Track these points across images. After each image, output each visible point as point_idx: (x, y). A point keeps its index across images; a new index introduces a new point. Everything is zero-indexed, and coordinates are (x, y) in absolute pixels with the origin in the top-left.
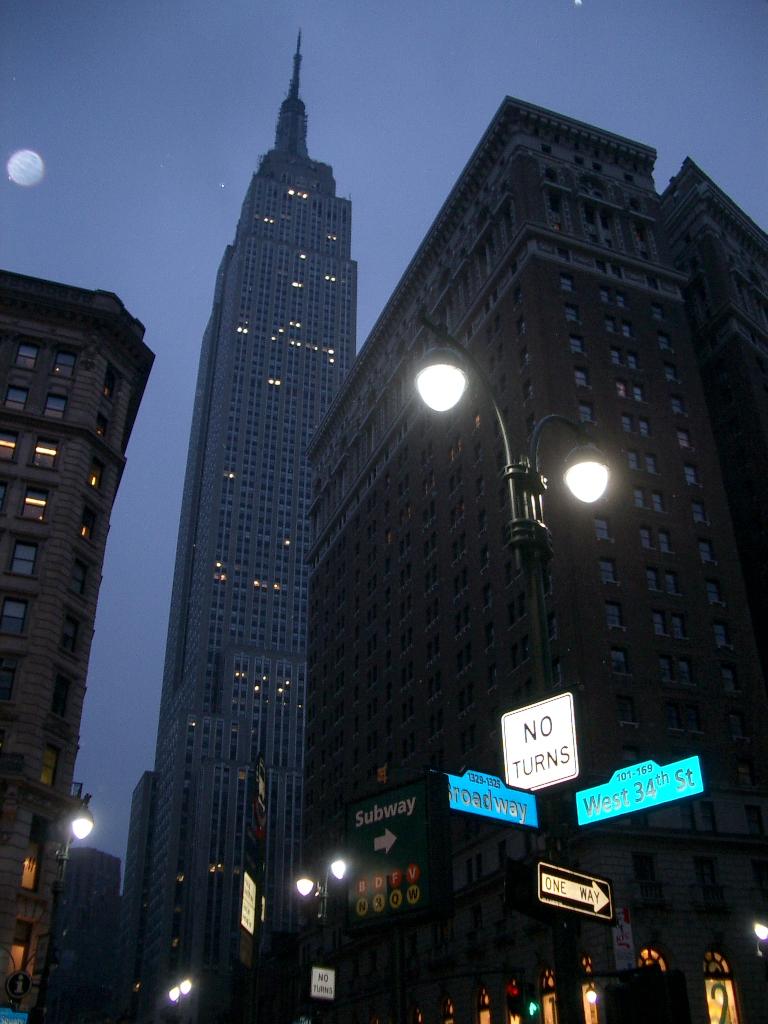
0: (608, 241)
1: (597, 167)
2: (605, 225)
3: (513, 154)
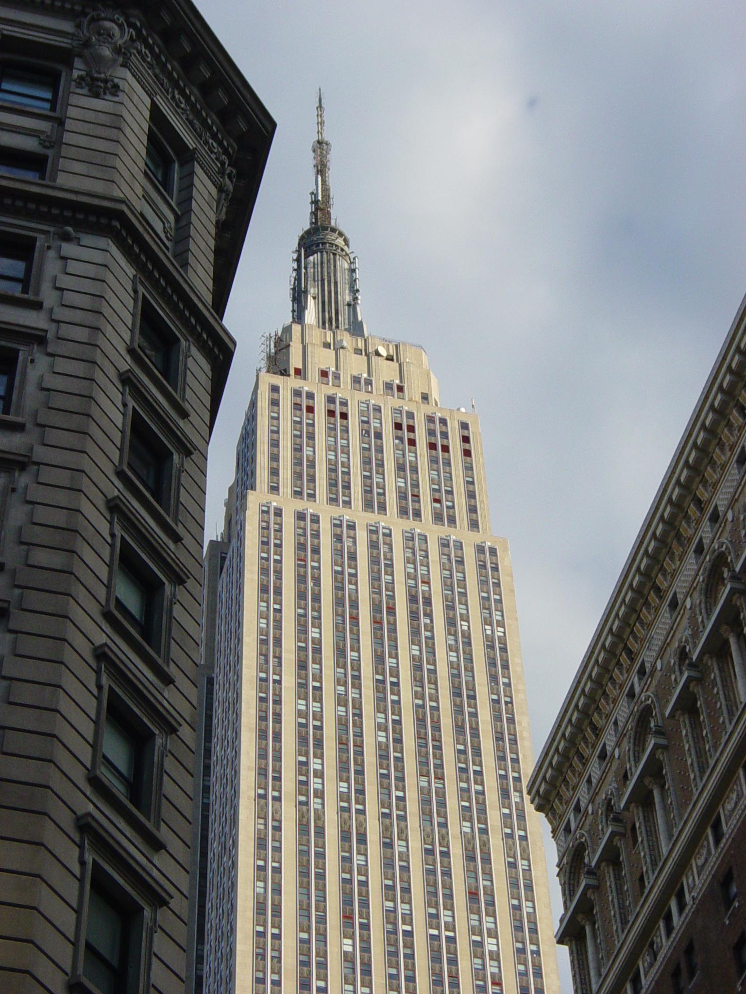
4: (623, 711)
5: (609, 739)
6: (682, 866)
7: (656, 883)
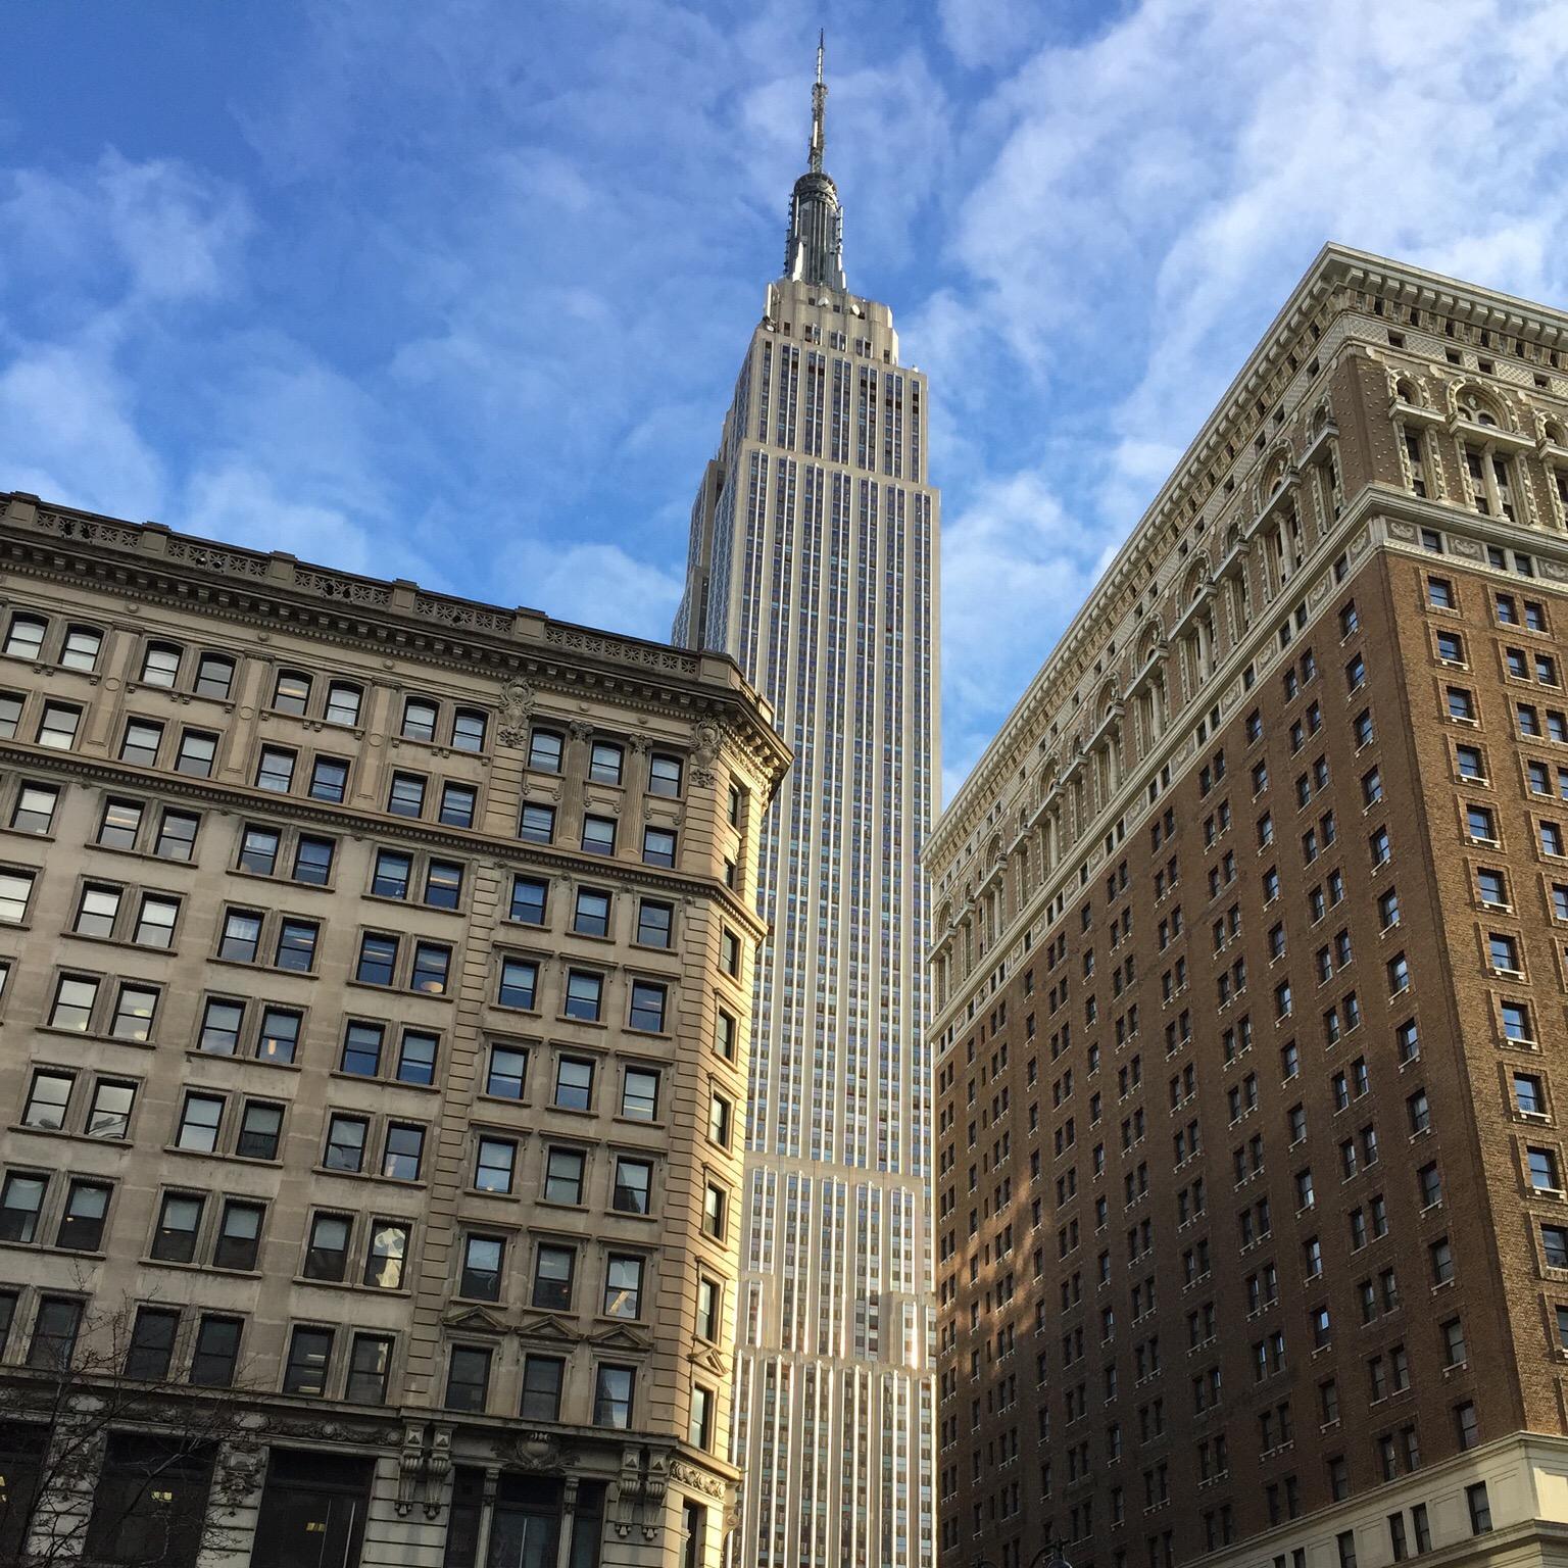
0: (1507, 509)
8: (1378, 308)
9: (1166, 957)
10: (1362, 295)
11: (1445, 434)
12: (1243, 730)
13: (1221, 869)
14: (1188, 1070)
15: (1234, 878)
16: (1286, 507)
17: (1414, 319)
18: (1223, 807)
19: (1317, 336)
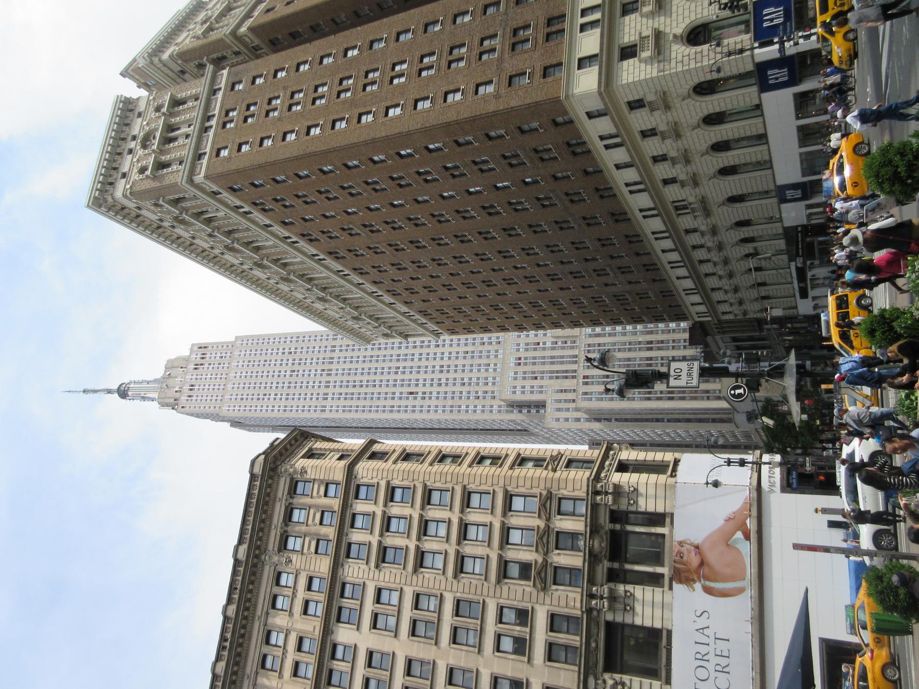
1: (134, 138)
2: (178, 129)
3: (130, 200)
4: (350, 323)
5: (356, 326)
6: (399, 312)
7: (401, 317)
8: (111, 184)
9: (389, 251)
10: (106, 191)
11: (161, 152)
12: (289, 227)
13: (349, 232)
14: (434, 239)
15: (351, 226)
16: (198, 215)
17: (115, 169)
18: (323, 232)
19: (125, 208)
